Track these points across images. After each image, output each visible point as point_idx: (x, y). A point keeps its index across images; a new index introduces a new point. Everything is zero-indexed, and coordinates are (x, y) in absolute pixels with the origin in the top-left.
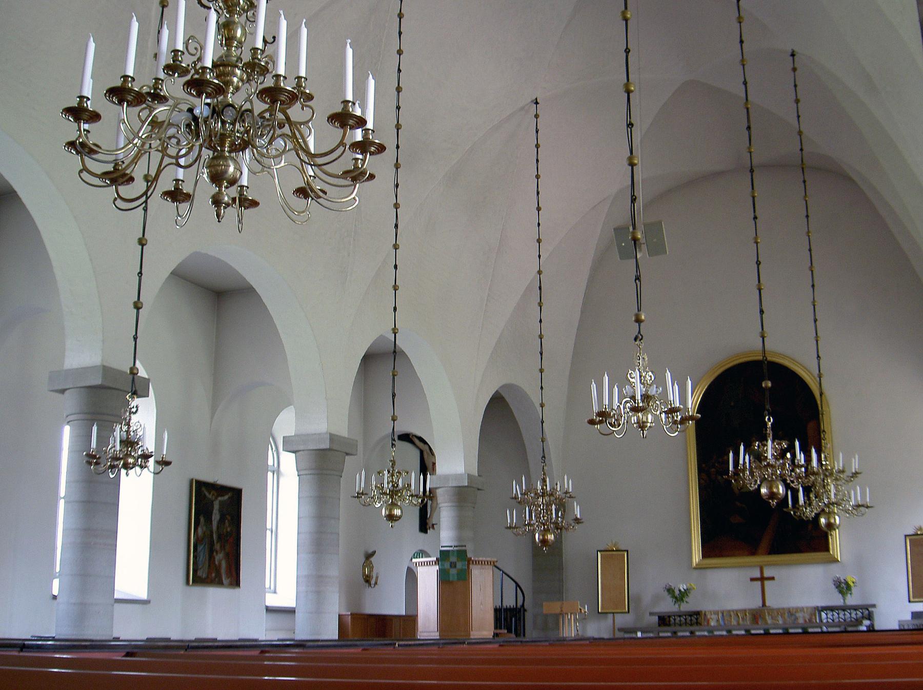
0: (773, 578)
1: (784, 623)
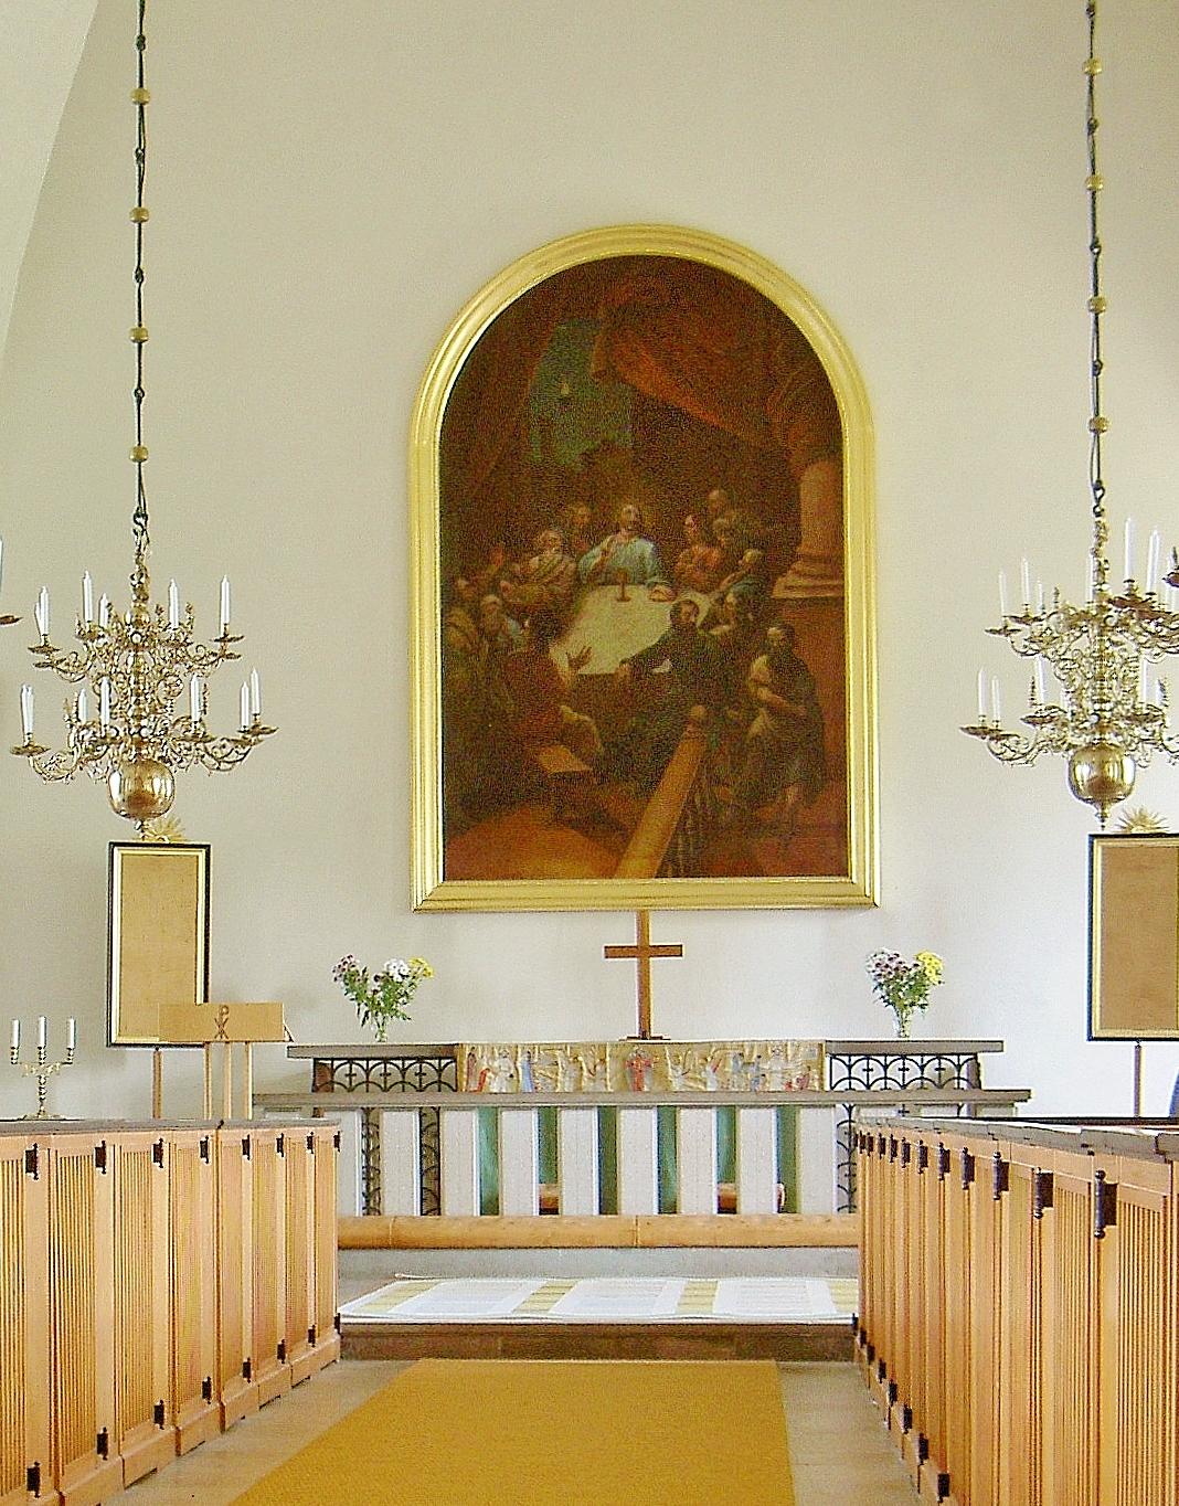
0: (675, 951)
1: (724, 1090)
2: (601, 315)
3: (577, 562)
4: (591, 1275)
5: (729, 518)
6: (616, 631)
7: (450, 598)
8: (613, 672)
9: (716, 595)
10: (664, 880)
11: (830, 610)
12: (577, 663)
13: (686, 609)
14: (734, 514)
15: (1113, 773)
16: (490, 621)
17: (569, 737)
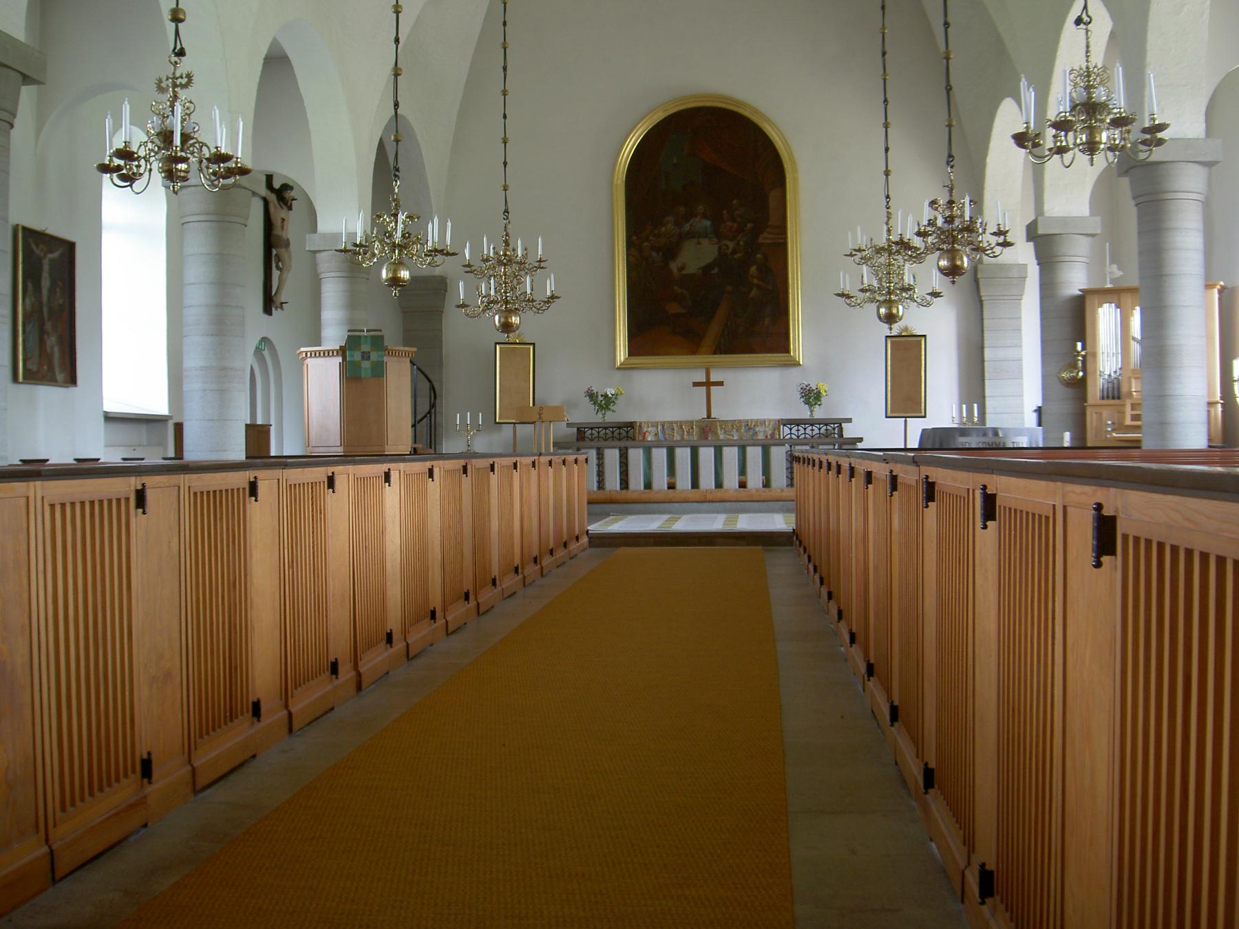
0: (721, 384)
1: (741, 439)
4: (688, 513)
6: (695, 256)
7: (630, 244)
11: (780, 249)
12: (682, 268)
15: (894, 311)
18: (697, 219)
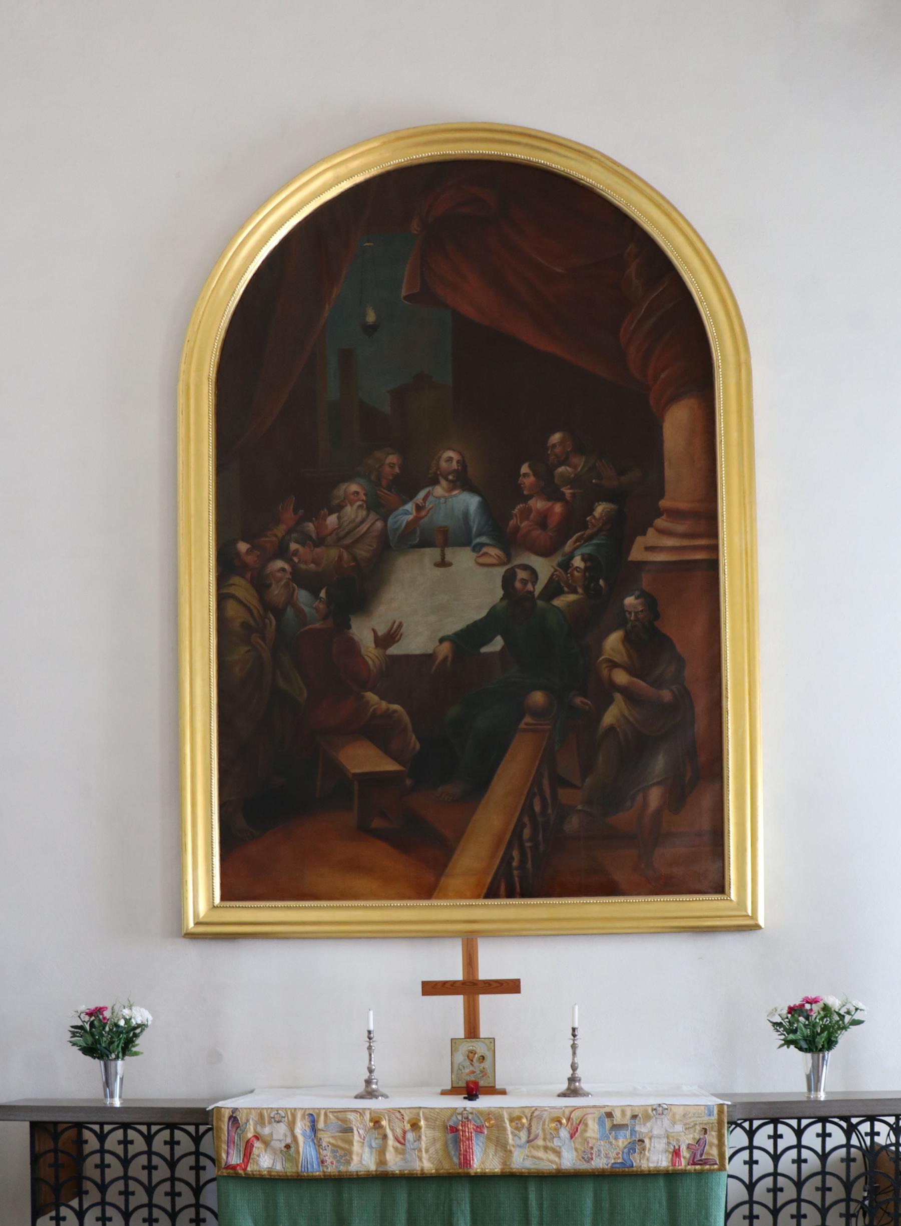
2: (415, 226)
3: (385, 520)
5: (575, 467)
6: (431, 604)
7: (227, 565)
8: (430, 652)
9: (558, 558)
10: (496, 902)
11: (700, 577)
13: (521, 574)
14: (579, 462)
16: (277, 592)
17: (379, 732)
18: (439, 490)
